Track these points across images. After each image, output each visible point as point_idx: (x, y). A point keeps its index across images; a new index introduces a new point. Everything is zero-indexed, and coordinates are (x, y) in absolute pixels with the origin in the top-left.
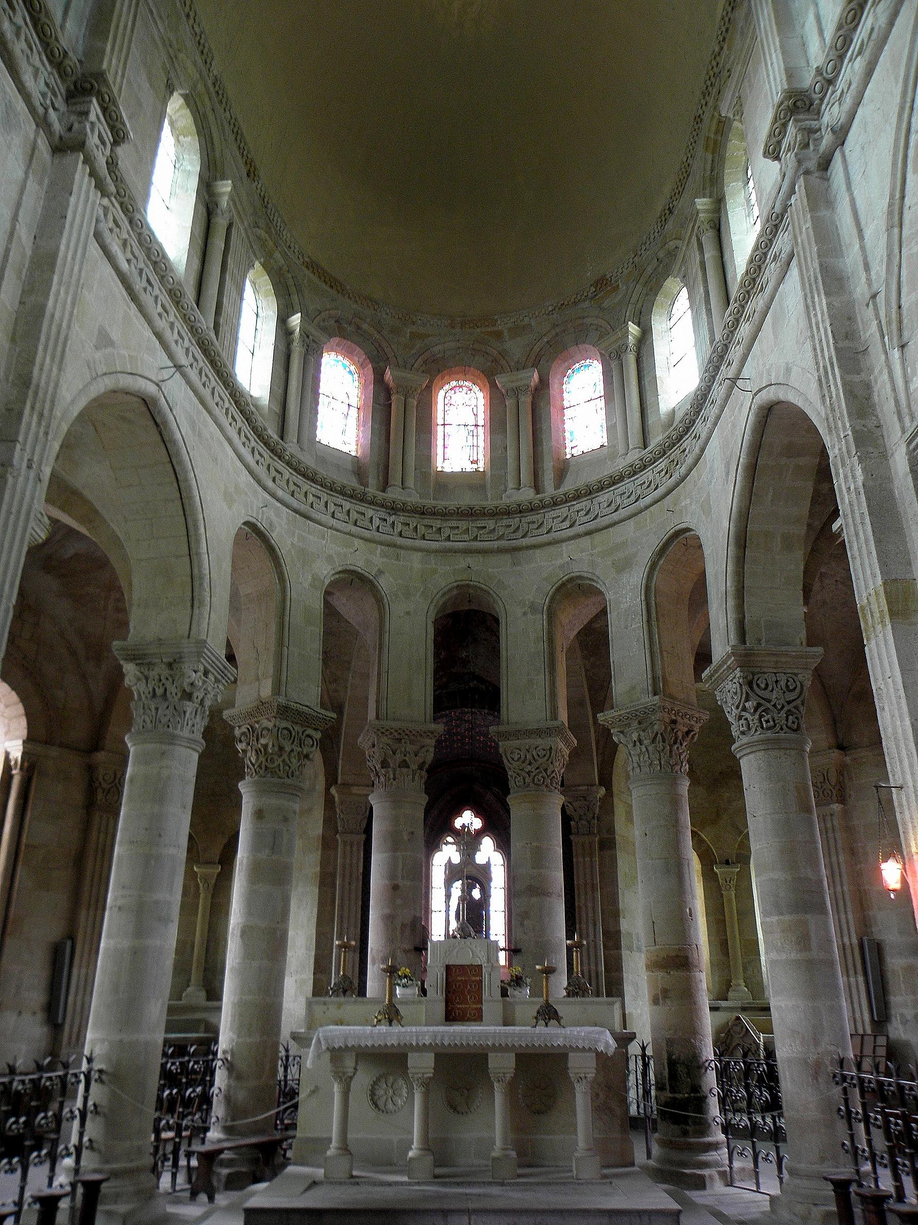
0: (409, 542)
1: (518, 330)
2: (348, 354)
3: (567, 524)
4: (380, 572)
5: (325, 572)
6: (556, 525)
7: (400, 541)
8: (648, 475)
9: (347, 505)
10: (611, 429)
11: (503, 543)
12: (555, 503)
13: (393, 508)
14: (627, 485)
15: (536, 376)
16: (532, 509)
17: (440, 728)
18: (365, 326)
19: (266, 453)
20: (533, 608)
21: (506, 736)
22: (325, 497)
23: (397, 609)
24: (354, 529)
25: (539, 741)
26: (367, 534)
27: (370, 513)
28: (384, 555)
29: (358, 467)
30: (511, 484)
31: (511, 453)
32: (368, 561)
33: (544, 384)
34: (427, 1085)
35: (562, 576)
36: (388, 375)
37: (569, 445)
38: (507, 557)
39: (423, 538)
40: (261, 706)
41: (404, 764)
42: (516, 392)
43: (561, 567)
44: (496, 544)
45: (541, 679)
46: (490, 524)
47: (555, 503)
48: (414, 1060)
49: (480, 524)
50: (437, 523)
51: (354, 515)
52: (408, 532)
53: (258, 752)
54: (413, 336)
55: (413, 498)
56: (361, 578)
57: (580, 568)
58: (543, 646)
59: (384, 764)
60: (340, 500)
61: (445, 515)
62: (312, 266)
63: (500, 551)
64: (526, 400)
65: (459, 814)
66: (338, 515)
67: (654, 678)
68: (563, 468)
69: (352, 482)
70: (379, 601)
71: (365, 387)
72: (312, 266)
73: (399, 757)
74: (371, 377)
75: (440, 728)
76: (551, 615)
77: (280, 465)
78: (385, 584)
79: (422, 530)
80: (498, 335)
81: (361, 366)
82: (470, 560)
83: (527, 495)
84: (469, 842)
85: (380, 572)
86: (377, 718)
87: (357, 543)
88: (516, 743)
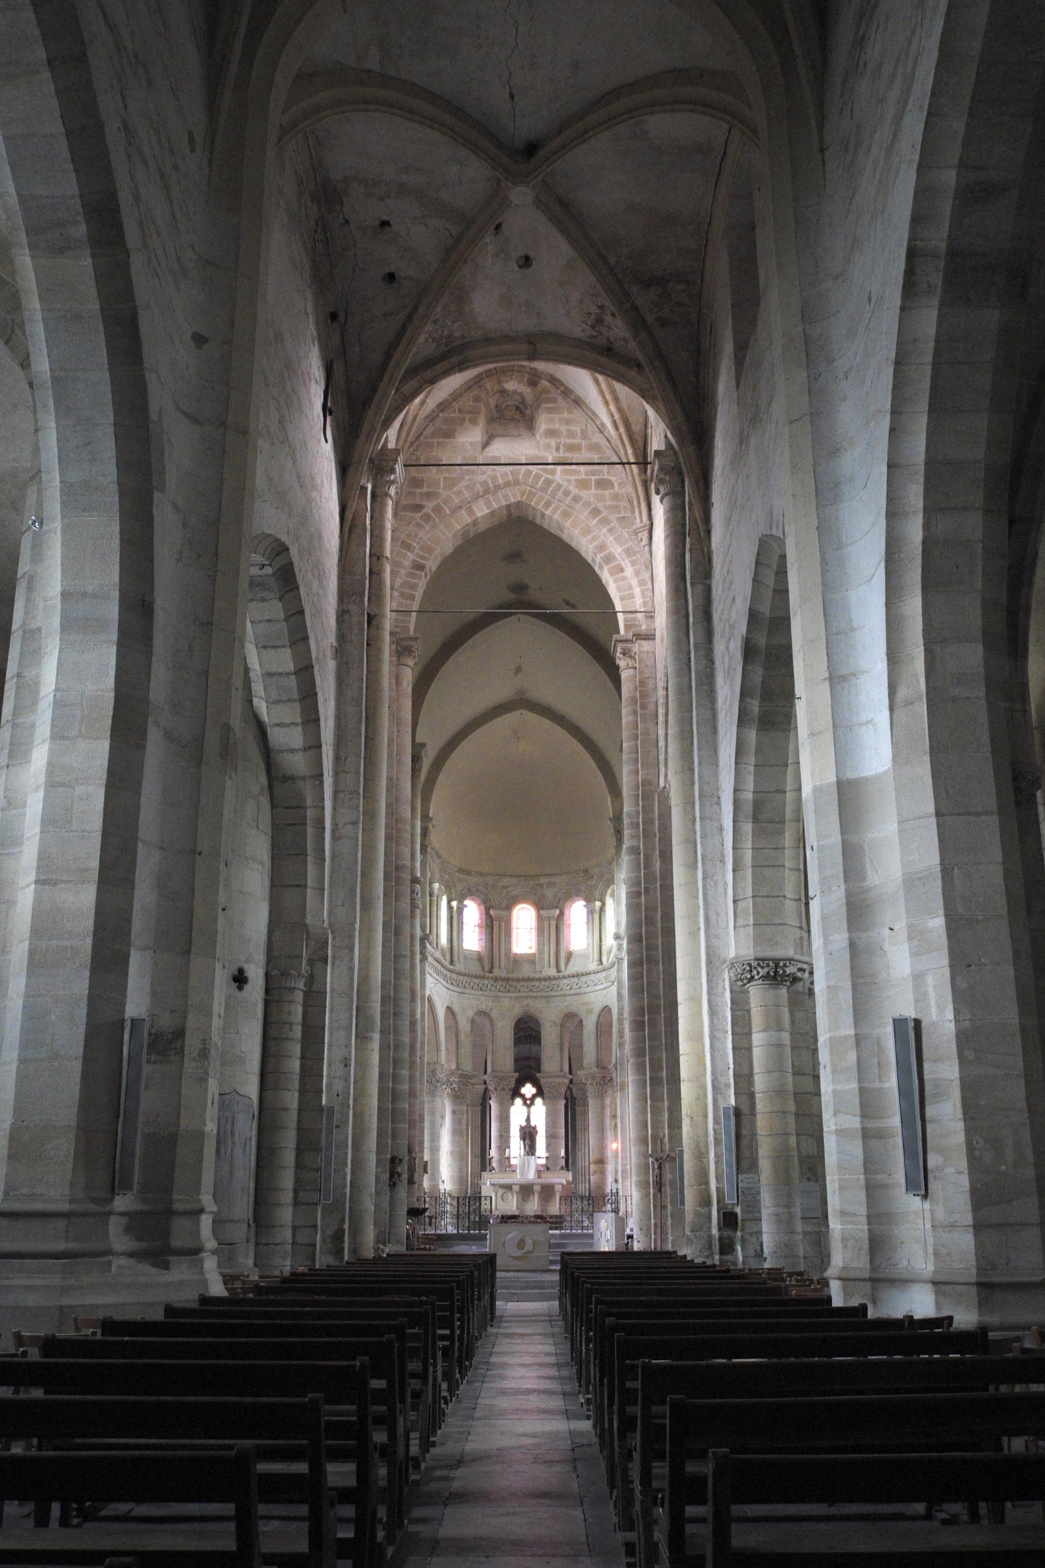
0: (502, 994)
1: (551, 885)
2: (474, 900)
3: (569, 988)
4: (491, 1009)
5: (470, 1013)
6: (565, 988)
7: (499, 994)
8: (598, 976)
9: (477, 982)
10: (588, 944)
11: (543, 994)
12: (564, 977)
13: (496, 979)
14: (592, 977)
15: (558, 912)
16: (555, 979)
17: (517, 1075)
18: (480, 888)
19: (448, 974)
20: (555, 1024)
21: (543, 1078)
22: (469, 980)
23: (499, 1025)
24: (481, 993)
25: (556, 1080)
26: (486, 993)
27: (486, 982)
28: (493, 1001)
29: (480, 958)
30: (546, 965)
31: (546, 949)
32: (487, 1006)
33: (562, 914)
34: (517, 1193)
35: (566, 1011)
36: (492, 912)
37: (572, 942)
38: (545, 1000)
39: (509, 991)
40: (452, 1073)
41: (503, 1089)
42: (549, 918)
43: (567, 1006)
44: (539, 994)
45: (557, 1054)
46: (537, 983)
47: (564, 977)
48: (514, 1187)
49: (533, 984)
50: (514, 983)
51: (480, 986)
52: (502, 989)
53: (452, 1090)
54: (504, 887)
55: (504, 975)
56: (484, 1013)
57: (573, 1009)
58: (557, 1041)
59: (496, 1089)
60: (475, 980)
61: (518, 980)
62: (461, 870)
63: (541, 997)
64: (553, 923)
65: (523, 1085)
66: (475, 987)
67: (598, 1060)
68: (569, 955)
69: (478, 972)
70: (491, 1021)
71: (481, 914)
72: (461, 870)
73: (501, 1086)
74: (484, 911)
75: (517, 1075)
76: (562, 1026)
77: (454, 976)
78: (494, 1014)
79: (508, 987)
80: (541, 885)
81: (479, 905)
82: (529, 1001)
83: (552, 972)
84: (529, 1103)
85: (491, 1009)
86: (493, 1071)
87: (482, 998)
88: (547, 1080)
